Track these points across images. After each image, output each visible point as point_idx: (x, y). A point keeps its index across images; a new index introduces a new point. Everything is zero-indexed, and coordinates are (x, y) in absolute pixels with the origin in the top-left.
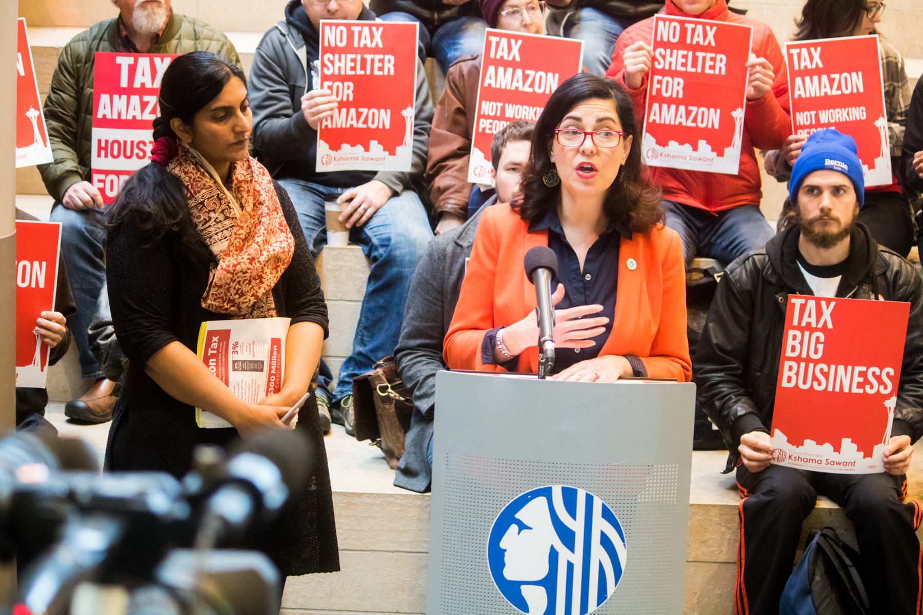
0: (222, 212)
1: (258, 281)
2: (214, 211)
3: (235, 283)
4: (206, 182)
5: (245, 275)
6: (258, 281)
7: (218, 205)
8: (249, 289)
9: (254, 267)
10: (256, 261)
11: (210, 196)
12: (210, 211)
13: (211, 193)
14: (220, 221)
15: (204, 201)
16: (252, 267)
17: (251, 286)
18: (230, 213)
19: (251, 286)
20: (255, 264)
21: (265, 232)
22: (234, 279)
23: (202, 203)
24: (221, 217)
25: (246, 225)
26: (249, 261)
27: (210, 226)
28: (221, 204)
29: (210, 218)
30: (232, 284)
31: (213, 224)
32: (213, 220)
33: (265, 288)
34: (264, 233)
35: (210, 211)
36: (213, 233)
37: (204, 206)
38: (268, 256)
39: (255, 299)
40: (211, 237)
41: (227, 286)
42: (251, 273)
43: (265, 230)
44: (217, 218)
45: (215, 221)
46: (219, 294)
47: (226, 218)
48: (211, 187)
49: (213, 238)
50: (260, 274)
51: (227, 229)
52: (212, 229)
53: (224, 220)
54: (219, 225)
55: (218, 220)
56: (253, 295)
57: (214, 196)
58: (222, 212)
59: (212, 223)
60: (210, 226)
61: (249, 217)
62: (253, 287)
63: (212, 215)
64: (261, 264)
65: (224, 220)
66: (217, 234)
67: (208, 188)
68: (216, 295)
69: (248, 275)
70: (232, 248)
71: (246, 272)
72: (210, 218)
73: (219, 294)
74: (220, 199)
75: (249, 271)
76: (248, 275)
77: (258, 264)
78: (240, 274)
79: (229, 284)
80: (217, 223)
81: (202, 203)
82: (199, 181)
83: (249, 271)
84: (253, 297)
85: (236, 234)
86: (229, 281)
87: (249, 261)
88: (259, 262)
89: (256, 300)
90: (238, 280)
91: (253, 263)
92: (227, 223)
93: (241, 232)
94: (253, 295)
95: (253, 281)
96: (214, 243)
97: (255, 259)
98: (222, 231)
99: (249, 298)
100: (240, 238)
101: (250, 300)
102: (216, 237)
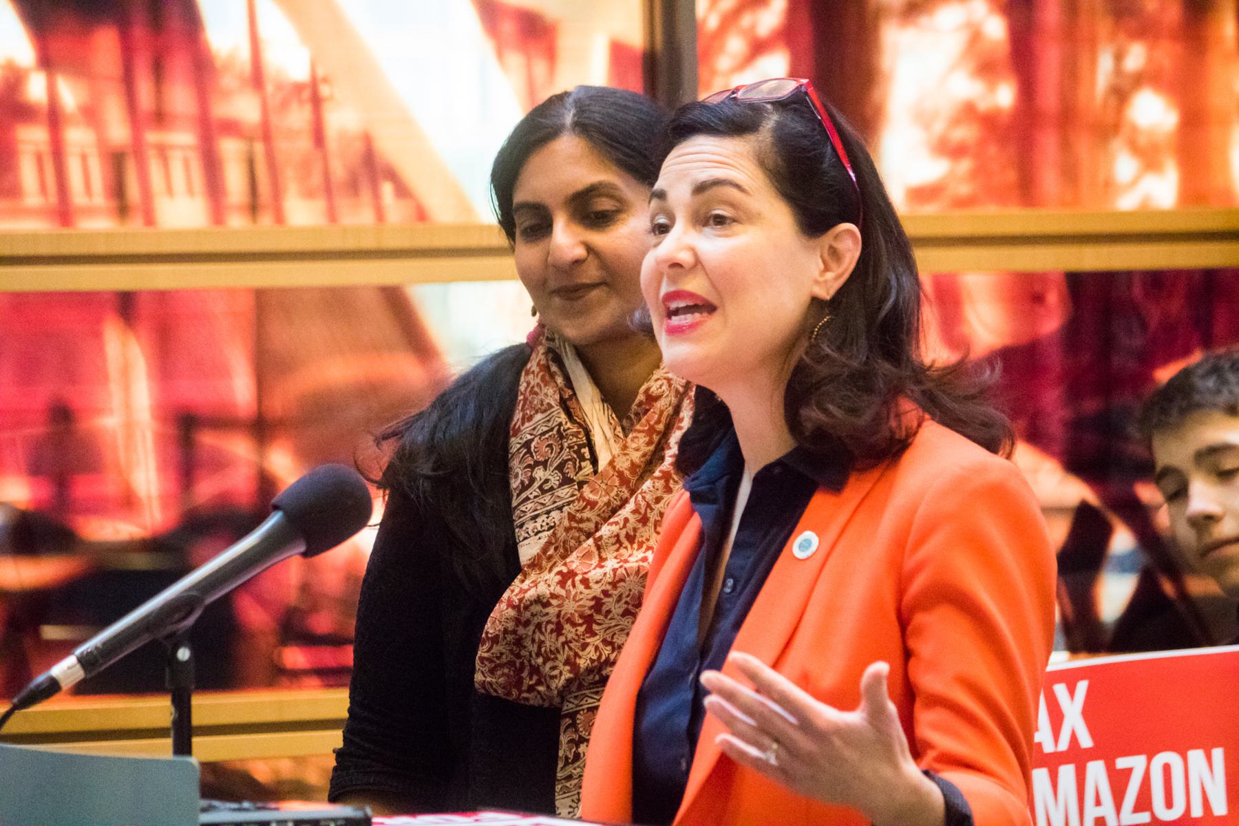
0: (560, 468)
1: (581, 629)
2: (544, 464)
3: (532, 628)
4: (546, 395)
5: (547, 610)
6: (581, 629)
7: (556, 448)
8: (559, 645)
9: (568, 592)
10: (578, 578)
11: (545, 429)
12: (537, 463)
13: (549, 421)
14: (552, 489)
15: (532, 440)
16: (563, 593)
17: (562, 639)
18: (580, 468)
19: (562, 639)
20: (574, 586)
21: (632, 518)
22: (523, 619)
23: (527, 444)
24: (555, 480)
25: (605, 499)
26: (558, 578)
27: (527, 499)
28: (562, 449)
29: (532, 480)
30: (521, 631)
31: (536, 494)
32: (536, 485)
33: (597, 648)
34: (626, 520)
35: (537, 463)
36: (529, 515)
37: (529, 452)
38: (615, 570)
39: (570, 672)
40: (521, 526)
41: (510, 638)
42: (559, 606)
43: (635, 512)
44: (547, 481)
45: (540, 487)
46: (498, 658)
47: (566, 481)
48: (550, 406)
49: (524, 528)
50: (589, 612)
51: (560, 509)
52: (529, 506)
53: (561, 485)
54: (547, 499)
55: (546, 487)
56: (567, 662)
57: (552, 430)
58: (560, 468)
59: (533, 491)
60: (527, 499)
61: (617, 484)
62: (567, 643)
63: (540, 473)
64: (588, 587)
65: (561, 485)
66: (534, 518)
67: (545, 411)
68: (490, 660)
69: (552, 611)
70: (551, 552)
71: (547, 604)
72: (532, 480)
73: (498, 658)
74: (561, 436)
75: (554, 602)
76: (552, 611)
77: (581, 587)
78: (536, 608)
79: (514, 632)
80: (543, 492)
81: (527, 444)
82: (536, 394)
83: (554, 602)
84: (568, 668)
85: (571, 517)
86: (511, 626)
87: (558, 578)
88: (585, 582)
89: (571, 676)
90: (536, 620)
91: (569, 582)
92: (565, 492)
93: (587, 514)
94: (567, 662)
95: (567, 627)
96: (525, 538)
97: (576, 574)
98: (548, 512)
99: (561, 667)
100: (580, 530)
101: (561, 673)
102: (530, 526)
